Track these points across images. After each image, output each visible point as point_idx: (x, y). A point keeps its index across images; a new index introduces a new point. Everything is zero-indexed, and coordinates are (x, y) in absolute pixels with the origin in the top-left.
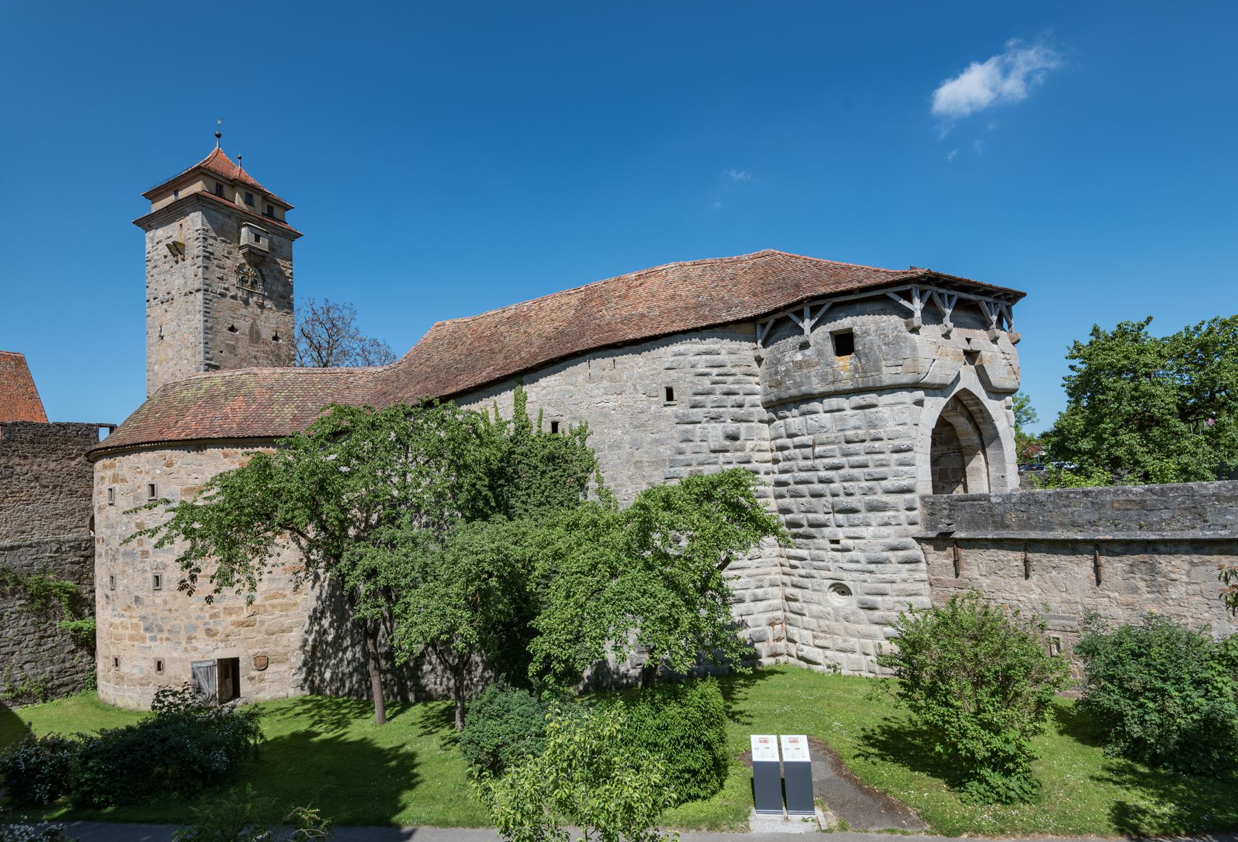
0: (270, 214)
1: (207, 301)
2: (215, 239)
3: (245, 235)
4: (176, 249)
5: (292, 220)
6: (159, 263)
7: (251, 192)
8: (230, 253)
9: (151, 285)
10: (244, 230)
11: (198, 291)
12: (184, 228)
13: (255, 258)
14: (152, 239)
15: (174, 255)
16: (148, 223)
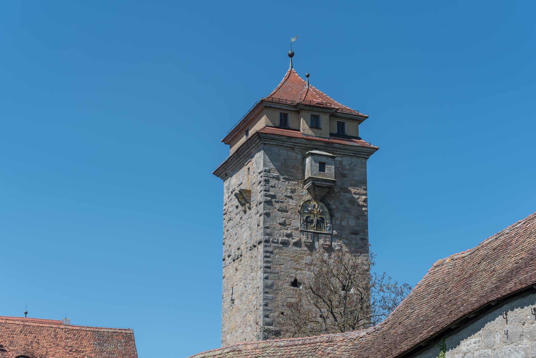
0: (341, 134)
1: (268, 254)
2: (278, 178)
3: (310, 167)
4: (243, 197)
5: (366, 134)
6: (233, 215)
7: (316, 112)
8: (293, 191)
9: (227, 242)
10: (308, 160)
11: (260, 243)
12: (251, 173)
13: (323, 191)
14: (228, 189)
15: (243, 205)
16: (224, 171)
